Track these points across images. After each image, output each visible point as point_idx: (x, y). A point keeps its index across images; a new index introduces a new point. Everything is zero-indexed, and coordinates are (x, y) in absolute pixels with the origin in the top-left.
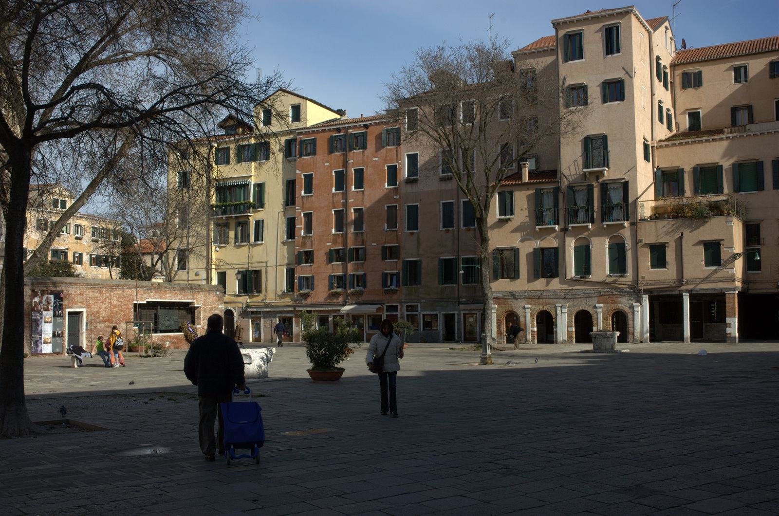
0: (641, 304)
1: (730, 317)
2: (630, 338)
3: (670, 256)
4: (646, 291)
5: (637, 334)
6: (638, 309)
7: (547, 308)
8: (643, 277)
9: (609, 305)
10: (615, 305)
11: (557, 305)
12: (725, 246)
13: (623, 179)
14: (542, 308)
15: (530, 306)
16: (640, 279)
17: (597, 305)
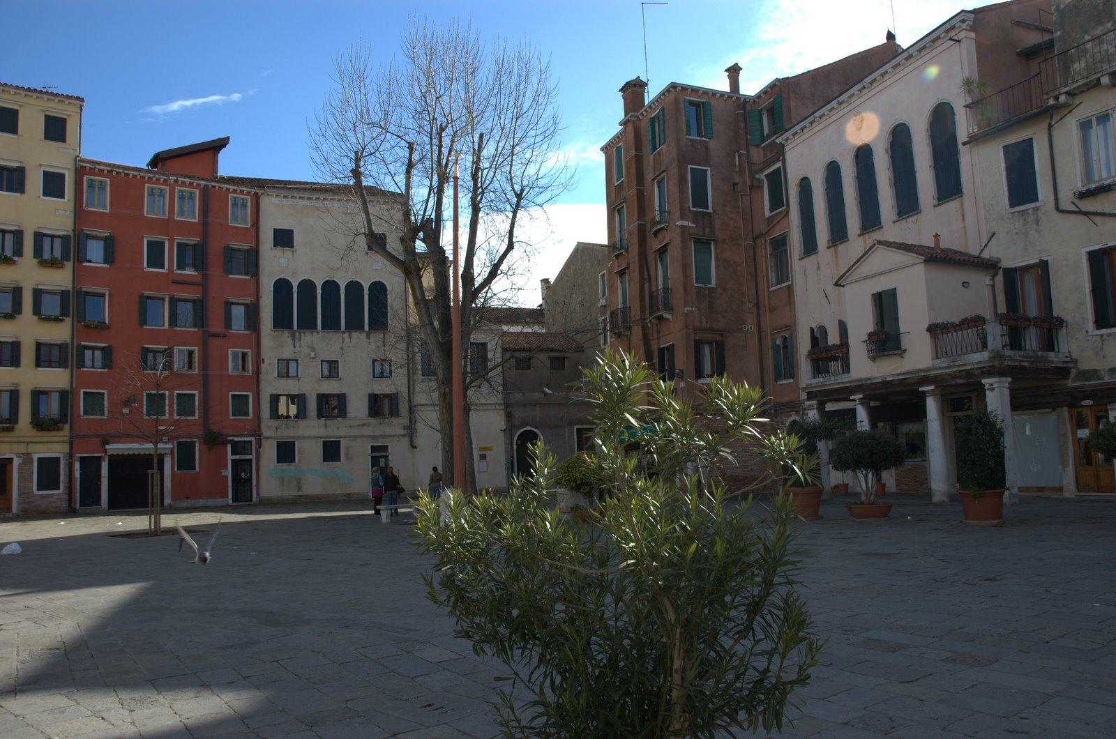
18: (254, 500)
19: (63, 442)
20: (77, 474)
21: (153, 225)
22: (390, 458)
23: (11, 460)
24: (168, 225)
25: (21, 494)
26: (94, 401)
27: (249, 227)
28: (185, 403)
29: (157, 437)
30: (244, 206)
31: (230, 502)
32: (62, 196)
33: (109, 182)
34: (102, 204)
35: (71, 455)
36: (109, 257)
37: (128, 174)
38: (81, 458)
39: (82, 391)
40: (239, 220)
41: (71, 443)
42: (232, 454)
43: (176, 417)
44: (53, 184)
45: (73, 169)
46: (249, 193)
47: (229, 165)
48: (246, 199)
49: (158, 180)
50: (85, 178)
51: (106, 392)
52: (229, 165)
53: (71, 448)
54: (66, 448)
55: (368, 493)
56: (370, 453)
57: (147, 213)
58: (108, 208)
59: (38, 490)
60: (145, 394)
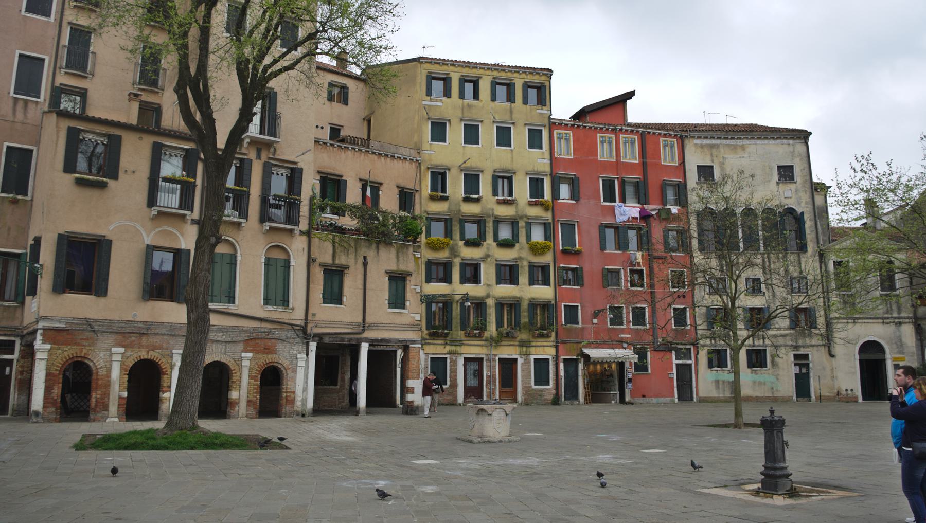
0: (307, 355)
1: (413, 378)
2: (286, 409)
3: (351, 285)
4: (316, 335)
5: (298, 403)
6: (301, 364)
7: (153, 355)
8: (314, 315)
9: (260, 356)
10: (269, 356)
11: (174, 351)
12: (412, 283)
13: (296, 163)
14: (144, 355)
15: (122, 350)
16: (310, 318)
17: (244, 355)
18: (695, 399)
19: (551, 346)
20: (562, 373)
21: (605, 166)
22: (811, 365)
23: (516, 359)
24: (618, 165)
25: (524, 388)
26: (571, 312)
27: (677, 165)
28: (639, 316)
29: (619, 343)
30: (672, 147)
31: (676, 400)
32: (541, 148)
33: (571, 134)
34: (565, 150)
35: (557, 357)
36: (575, 195)
37: (585, 127)
38: (564, 359)
39: (563, 304)
40: (667, 157)
41: (556, 347)
42: (676, 359)
43: (631, 326)
44: (535, 139)
45: (548, 126)
46: (676, 136)
47: (636, 113)
48: (674, 142)
49: (607, 129)
50: (555, 132)
51: (579, 305)
52: (636, 113)
53: (557, 351)
54: (553, 351)
55: (792, 397)
56: (793, 360)
57: (601, 158)
58: (572, 155)
59: (535, 385)
60: (631, 308)
